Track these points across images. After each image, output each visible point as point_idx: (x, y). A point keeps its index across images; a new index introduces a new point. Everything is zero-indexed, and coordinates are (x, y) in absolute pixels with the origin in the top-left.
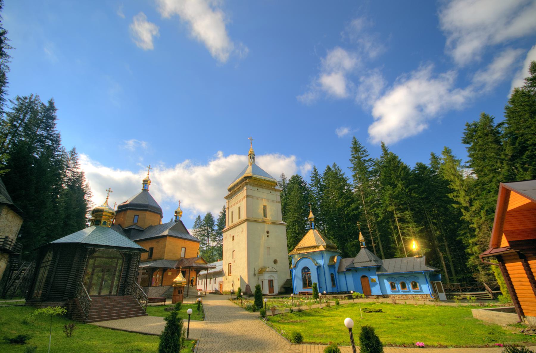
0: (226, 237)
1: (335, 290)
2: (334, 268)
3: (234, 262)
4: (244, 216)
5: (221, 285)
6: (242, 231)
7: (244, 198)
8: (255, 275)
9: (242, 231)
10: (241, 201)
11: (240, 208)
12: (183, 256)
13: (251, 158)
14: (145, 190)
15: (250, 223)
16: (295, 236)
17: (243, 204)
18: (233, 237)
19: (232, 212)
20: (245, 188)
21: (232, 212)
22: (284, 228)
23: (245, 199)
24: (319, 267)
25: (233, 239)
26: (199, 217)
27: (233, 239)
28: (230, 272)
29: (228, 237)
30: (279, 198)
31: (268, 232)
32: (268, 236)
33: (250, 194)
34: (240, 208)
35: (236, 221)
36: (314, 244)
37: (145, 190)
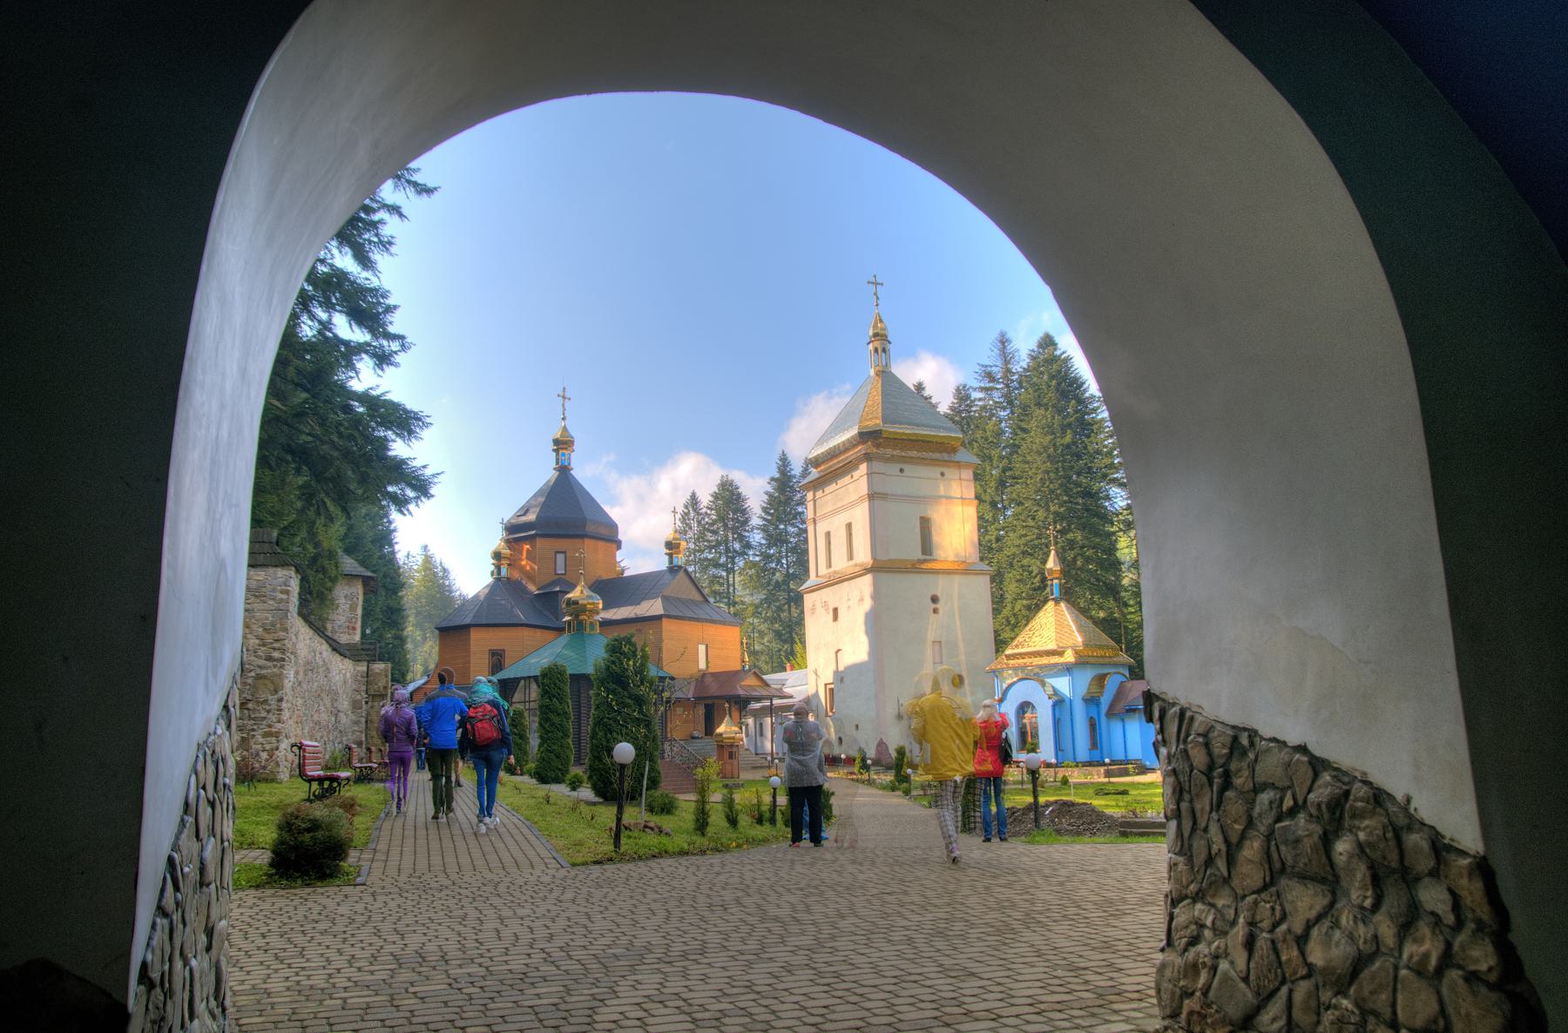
0: (813, 609)
1: (1096, 755)
2: (1098, 704)
4: (863, 555)
7: (861, 499)
8: (900, 717)
10: (852, 505)
11: (849, 526)
12: (702, 665)
13: (876, 350)
14: (564, 470)
15: (884, 577)
16: (1009, 621)
17: (860, 516)
18: (835, 610)
19: (828, 534)
20: (863, 468)
21: (828, 534)
22: (988, 578)
23: (866, 504)
24: (1059, 702)
25: (835, 618)
26: (694, 501)
27: (835, 618)
29: (819, 610)
33: (879, 489)
34: (849, 526)
35: (840, 563)
36: (1052, 646)
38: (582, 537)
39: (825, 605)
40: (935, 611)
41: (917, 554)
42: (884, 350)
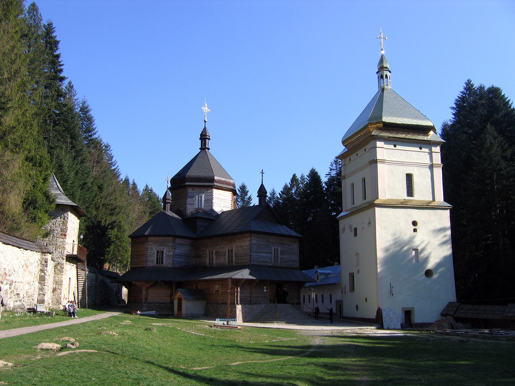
0: (344, 229)
3: (358, 272)
5: (340, 304)
6: (369, 223)
9: (369, 223)
18: (356, 229)
21: (353, 185)
25: (356, 235)
28: (352, 288)
29: (348, 230)
30: (437, 158)
31: (415, 223)
32: (415, 230)
34: (364, 180)
35: (359, 201)
37: (204, 148)
38: (212, 187)
39: (351, 227)
40: (415, 230)
41: (403, 195)
42: (386, 75)
